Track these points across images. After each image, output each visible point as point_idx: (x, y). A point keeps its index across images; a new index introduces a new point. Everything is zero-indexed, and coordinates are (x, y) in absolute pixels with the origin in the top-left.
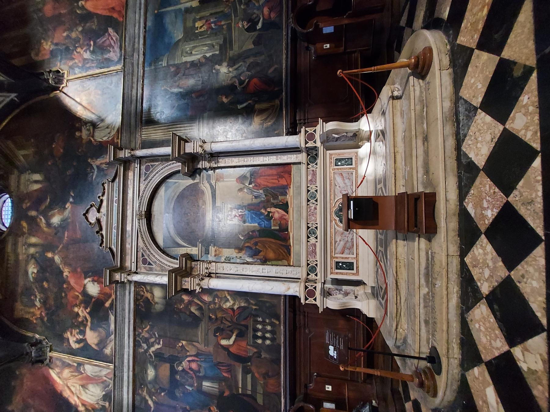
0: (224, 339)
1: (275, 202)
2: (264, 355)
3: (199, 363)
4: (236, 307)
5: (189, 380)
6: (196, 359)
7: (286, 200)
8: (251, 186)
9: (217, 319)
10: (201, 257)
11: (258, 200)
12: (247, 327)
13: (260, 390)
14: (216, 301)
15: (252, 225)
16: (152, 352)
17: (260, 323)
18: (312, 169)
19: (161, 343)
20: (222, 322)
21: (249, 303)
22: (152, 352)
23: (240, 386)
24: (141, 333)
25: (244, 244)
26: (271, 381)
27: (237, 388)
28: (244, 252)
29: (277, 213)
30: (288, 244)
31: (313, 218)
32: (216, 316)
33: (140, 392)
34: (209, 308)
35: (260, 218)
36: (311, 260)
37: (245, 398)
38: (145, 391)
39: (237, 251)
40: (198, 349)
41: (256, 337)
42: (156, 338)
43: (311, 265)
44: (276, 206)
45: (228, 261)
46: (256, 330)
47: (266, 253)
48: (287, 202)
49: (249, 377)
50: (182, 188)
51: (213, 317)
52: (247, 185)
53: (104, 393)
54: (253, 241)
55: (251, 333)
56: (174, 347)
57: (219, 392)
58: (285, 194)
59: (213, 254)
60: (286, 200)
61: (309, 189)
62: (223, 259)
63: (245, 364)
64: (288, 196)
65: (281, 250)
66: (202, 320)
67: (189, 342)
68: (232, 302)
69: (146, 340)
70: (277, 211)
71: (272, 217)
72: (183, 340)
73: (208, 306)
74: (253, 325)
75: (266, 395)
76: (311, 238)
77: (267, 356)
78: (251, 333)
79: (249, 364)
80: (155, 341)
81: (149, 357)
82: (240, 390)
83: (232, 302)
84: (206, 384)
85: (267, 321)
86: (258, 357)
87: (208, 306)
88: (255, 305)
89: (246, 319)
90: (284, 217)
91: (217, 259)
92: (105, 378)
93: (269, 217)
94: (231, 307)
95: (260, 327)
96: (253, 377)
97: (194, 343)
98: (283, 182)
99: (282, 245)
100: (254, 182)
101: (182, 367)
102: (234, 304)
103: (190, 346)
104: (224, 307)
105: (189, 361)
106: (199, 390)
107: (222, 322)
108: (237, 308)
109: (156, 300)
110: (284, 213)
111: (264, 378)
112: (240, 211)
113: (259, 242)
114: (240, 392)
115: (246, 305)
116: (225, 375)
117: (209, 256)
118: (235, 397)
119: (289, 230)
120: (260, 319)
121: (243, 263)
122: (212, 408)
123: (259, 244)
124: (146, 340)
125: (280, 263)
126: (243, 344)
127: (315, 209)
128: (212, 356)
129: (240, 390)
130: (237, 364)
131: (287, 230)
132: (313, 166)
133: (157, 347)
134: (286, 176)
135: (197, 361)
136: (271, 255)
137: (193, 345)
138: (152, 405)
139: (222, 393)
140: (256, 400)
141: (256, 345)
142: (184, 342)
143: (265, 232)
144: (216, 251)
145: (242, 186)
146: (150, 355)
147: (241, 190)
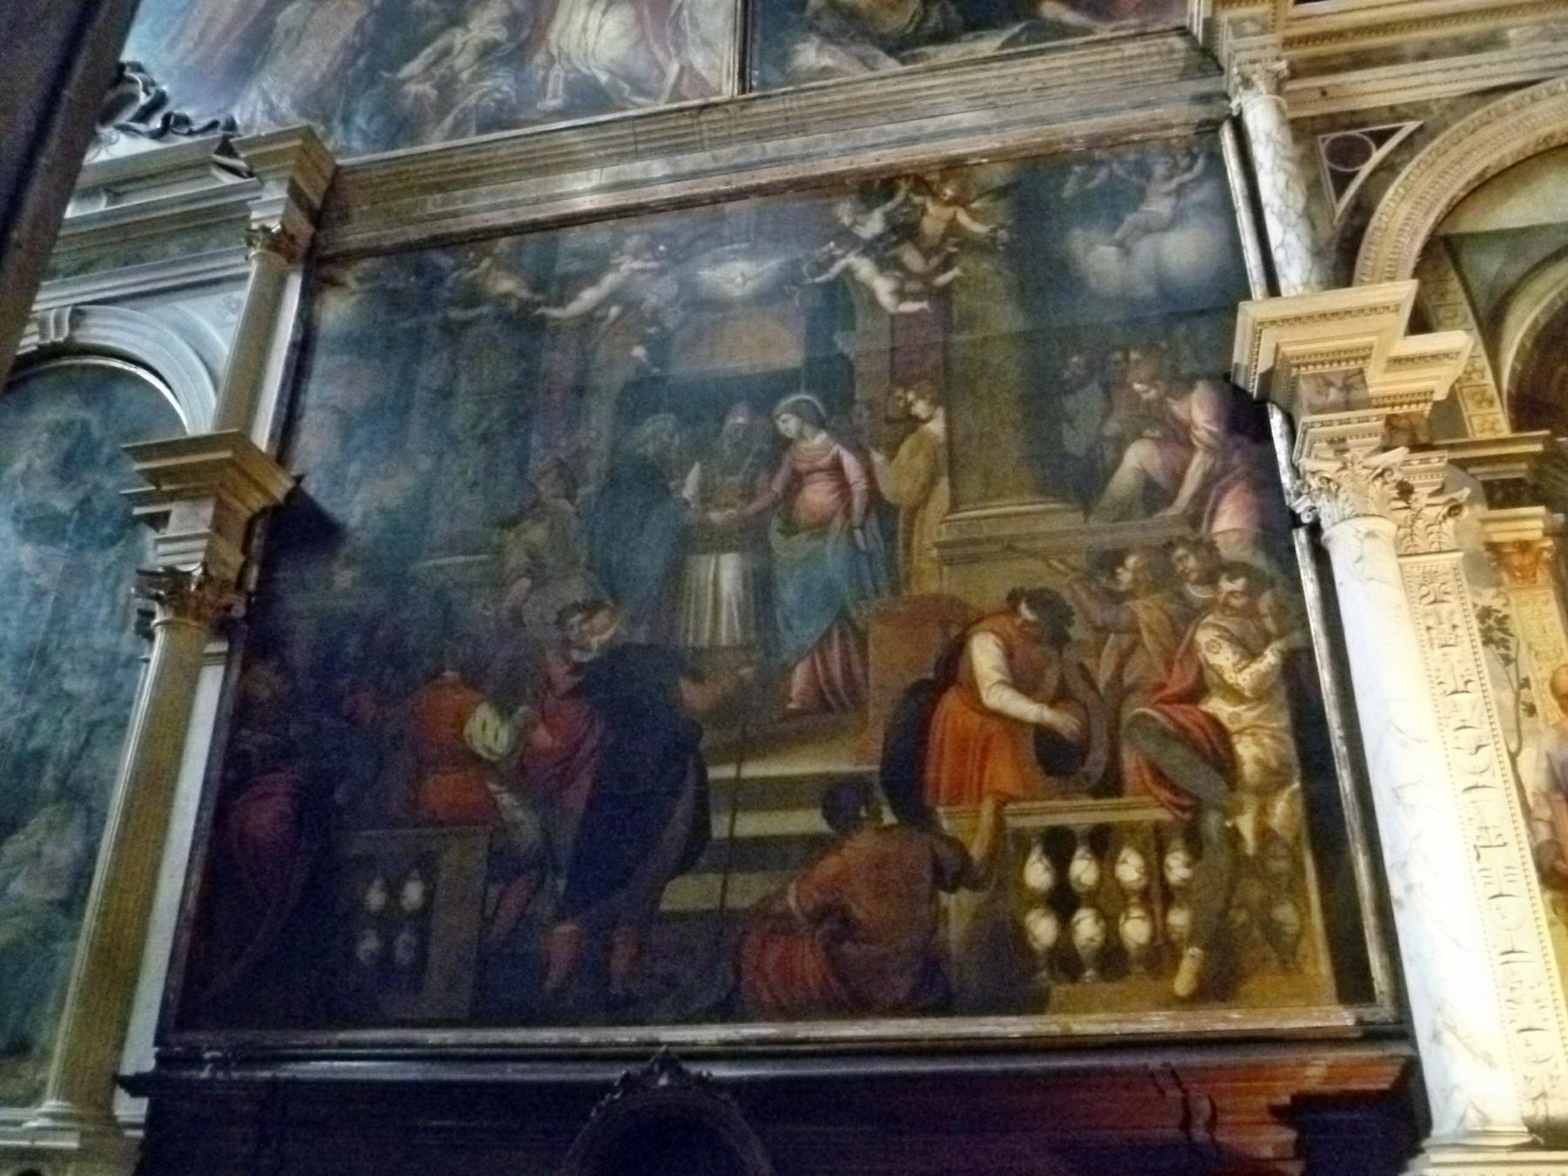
0: (1009, 655)
2: (959, 905)
3: (838, 521)
4: (1217, 706)
5: (735, 480)
6: (858, 503)
9: (1117, 598)
12: (1111, 785)
13: (746, 891)
14: (1226, 585)
16: (848, 271)
17: (1155, 869)
19: (910, 307)
20: (1102, 630)
21: (1266, 792)
22: (848, 271)
23: (752, 770)
24: (935, 196)
26: (809, 961)
27: (740, 752)
32: (1131, 594)
33: (632, 242)
34: (1170, 546)
37: (683, 809)
38: (637, 265)
40: (913, 511)
41: (1059, 846)
42: (925, 278)
46: (1103, 843)
49: (809, 821)
51: (1125, 577)
53: (604, 78)
55: (1081, 814)
56: (901, 377)
57: (698, 652)
59: (1504, 533)
62: (1489, 598)
63: (879, 794)
66: (1087, 510)
67: (943, 452)
68: (1244, 679)
69: (904, 230)
72: (949, 421)
73: (1183, 540)
74: (1133, 828)
75: (722, 919)
77: (956, 930)
78: (1081, 814)
79: (889, 818)
80: (910, 275)
81: (820, 253)
82: (728, 772)
83: (1244, 679)
84: (726, 573)
85: (1179, 919)
86: (938, 870)
87: (1183, 540)
88: (1265, 834)
89: (1159, 775)
92: (674, 68)
94: (1210, 676)
95: (1130, 869)
96: (815, 845)
97: (944, 484)
101: (801, 436)
102: (1234, 694)
103: (921, 463)
104: (1204, 637)
105: (837, 468)
106: (693, 540)
107: (1102, 630)
108: (1214, 721)
109: (1144, 249)
111: (821, 914)
114: (718, 772)
115: (1249, 770)
116: (799, 678)
117: (1481, 510)
118: (683, 750)
120: (1177, 868)
122: (600, 619)
124: (904, 230)
126: (1003, 773)
128: (895, 590)
129: (728, 772)
130: (874, 740)
133: (883, 288)
135: (848, 513)
137: (932, 481)
138: (574, 308)
139: (694, 665)
140: (686, 864)
141: (1010, 848)
142: (936, 427)
144: (1524, 546)
146: (833, 259)
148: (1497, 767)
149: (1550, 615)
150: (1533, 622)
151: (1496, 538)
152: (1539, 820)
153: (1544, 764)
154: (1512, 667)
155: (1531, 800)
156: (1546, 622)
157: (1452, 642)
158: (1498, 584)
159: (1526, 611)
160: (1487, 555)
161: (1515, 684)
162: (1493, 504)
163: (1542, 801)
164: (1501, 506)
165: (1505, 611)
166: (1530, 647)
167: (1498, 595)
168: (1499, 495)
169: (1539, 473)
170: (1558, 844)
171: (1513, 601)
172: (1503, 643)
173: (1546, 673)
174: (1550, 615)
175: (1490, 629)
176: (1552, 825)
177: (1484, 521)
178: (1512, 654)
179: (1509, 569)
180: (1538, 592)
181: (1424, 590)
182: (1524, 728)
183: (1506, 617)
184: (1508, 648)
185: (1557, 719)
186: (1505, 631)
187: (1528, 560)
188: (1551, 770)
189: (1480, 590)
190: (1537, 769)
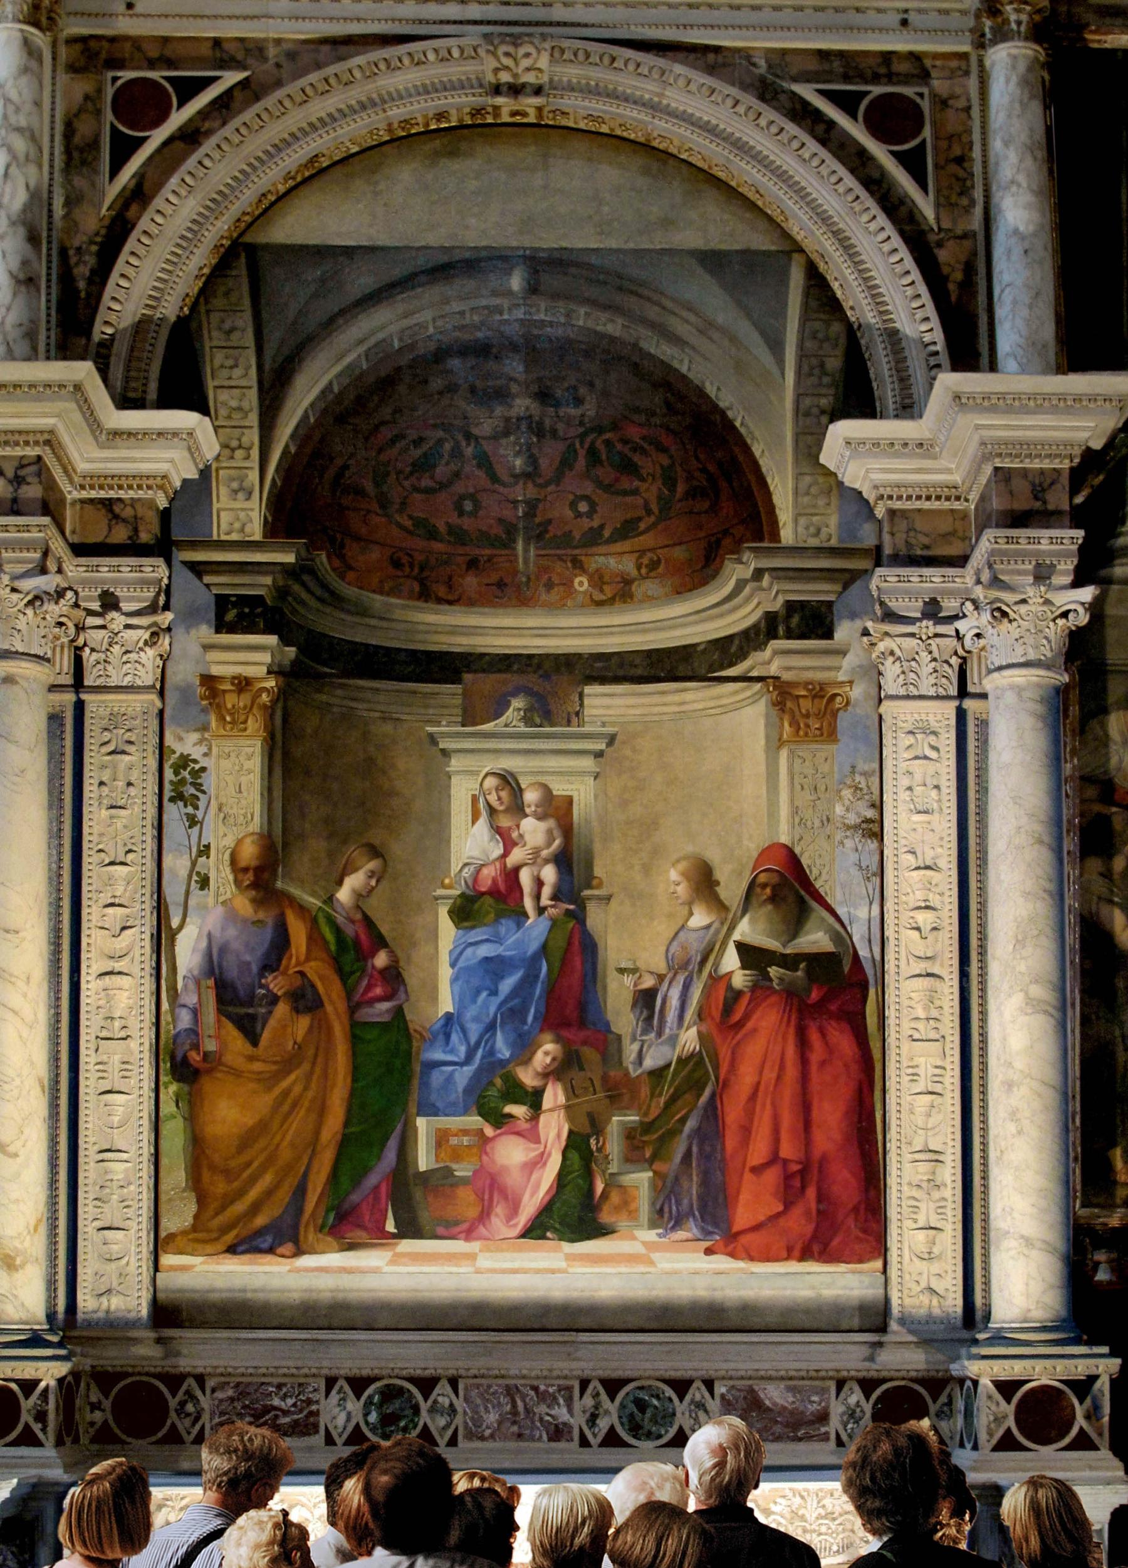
1: (613, 1144)
7: (623, 1224)
8: (731, 961)
10: (198, 569)
11: (621, 1015)
15: (445, 973)
18: (837, 1409)
25: (302, 910)
28: (244, 905)
29: (529, 1160)
30: (311, 1236)
31: (492, 1417)
35: (491, 1027)
36: (205, 1402)
39: (249, 853)
43: (173, 1403)
44: (581, 1149)
45: (179, 785)
47: (237, 1074)
48: (601, 1231)
50: (726, 395)
52: (745, 930)
54: (318, 971)
58: (667, 1215)
59: (224, 665)
60: (623, 1224)
61: (697, 1392)
62: (185, 743)
64: (651, 1235)
65: (267, 1179)
70: (541, 1160)
71: (500, 1120)
76: (354, 1406)
90: (500, 1210)
91: (185, 692)
93: (499, 1097)
98: (754, 1200)
99: (301, 1191)
100: (760, 987)
110: (530, 1206)
112: (549, 874)
113: (321, 1027)
117: (205, 632)
119: (407, 1245)
121: (160, 908)
123: (304, 1023)
125: (176, 1176)
127: (558, 1433)
131: (410, 1229)
132: (852, 1415)
134: (799, 1223)
136: (229, 1112)
143: (389, 1069)
144: (243, 684)
145: (732, 889)
147: (704, 881)
148: (137, 952)
149: (250, 772)
150: (228, 778)
151: (215, 670)
152: (184, 1006)
153: (204, 944)
154: (196, 829)
155: (180, 985)
156: (244, 780)
157: (121, 803)
158: (205, 728)
159: (225, 764)
160: (200, 691)
161: (194, 850)
162: (221, 626)
163: (192, 986)
164: (232, 629)
165: (204, 762)
166: (220, 809)
167: (200, 742)
168: (231, 615)
169: (282, 593)
170: (197, 1034)
171: (215, 750)
172: (193, 801)
173: (229, 841)
174: (250, 772)
175: (183, 782)
176: (195, 1012)
177: (207, 647)
178: (200, 815)
179: (219, 709)
180: (243, 742)
181: (107, 736)
182: (192, 902)
183: (203, 769)
184: (196, 808)
185: (229, 895)
186: (198, 786)
187: (245, 700)
188: (209, 954)
189: (183, 735)
190: (194, 950)
